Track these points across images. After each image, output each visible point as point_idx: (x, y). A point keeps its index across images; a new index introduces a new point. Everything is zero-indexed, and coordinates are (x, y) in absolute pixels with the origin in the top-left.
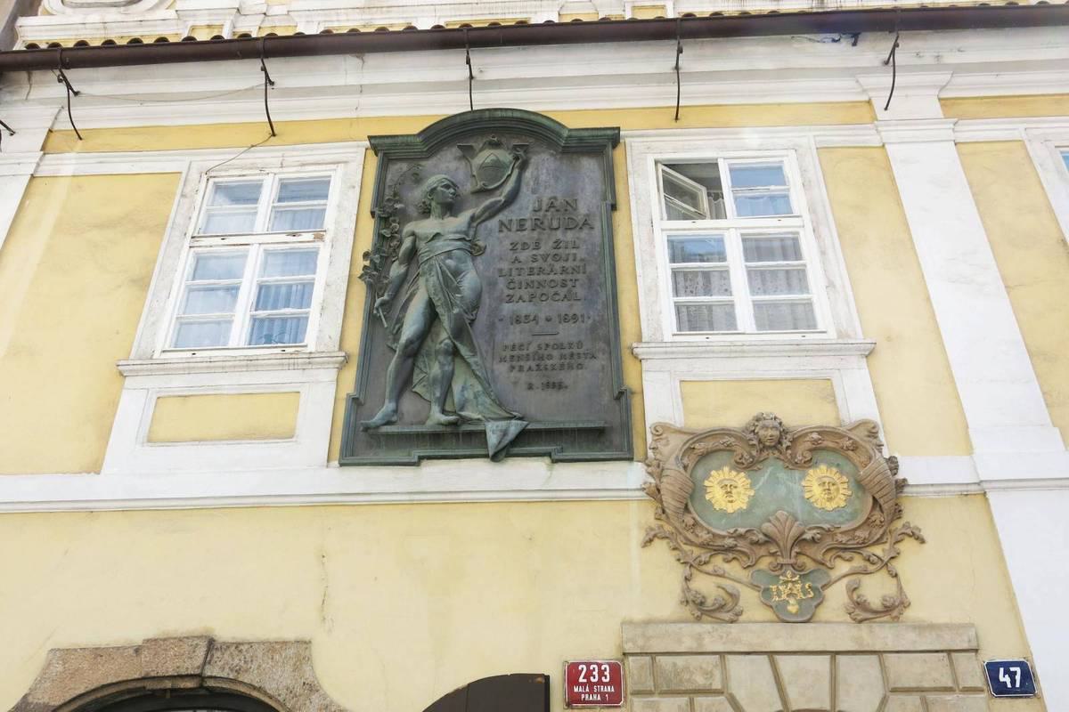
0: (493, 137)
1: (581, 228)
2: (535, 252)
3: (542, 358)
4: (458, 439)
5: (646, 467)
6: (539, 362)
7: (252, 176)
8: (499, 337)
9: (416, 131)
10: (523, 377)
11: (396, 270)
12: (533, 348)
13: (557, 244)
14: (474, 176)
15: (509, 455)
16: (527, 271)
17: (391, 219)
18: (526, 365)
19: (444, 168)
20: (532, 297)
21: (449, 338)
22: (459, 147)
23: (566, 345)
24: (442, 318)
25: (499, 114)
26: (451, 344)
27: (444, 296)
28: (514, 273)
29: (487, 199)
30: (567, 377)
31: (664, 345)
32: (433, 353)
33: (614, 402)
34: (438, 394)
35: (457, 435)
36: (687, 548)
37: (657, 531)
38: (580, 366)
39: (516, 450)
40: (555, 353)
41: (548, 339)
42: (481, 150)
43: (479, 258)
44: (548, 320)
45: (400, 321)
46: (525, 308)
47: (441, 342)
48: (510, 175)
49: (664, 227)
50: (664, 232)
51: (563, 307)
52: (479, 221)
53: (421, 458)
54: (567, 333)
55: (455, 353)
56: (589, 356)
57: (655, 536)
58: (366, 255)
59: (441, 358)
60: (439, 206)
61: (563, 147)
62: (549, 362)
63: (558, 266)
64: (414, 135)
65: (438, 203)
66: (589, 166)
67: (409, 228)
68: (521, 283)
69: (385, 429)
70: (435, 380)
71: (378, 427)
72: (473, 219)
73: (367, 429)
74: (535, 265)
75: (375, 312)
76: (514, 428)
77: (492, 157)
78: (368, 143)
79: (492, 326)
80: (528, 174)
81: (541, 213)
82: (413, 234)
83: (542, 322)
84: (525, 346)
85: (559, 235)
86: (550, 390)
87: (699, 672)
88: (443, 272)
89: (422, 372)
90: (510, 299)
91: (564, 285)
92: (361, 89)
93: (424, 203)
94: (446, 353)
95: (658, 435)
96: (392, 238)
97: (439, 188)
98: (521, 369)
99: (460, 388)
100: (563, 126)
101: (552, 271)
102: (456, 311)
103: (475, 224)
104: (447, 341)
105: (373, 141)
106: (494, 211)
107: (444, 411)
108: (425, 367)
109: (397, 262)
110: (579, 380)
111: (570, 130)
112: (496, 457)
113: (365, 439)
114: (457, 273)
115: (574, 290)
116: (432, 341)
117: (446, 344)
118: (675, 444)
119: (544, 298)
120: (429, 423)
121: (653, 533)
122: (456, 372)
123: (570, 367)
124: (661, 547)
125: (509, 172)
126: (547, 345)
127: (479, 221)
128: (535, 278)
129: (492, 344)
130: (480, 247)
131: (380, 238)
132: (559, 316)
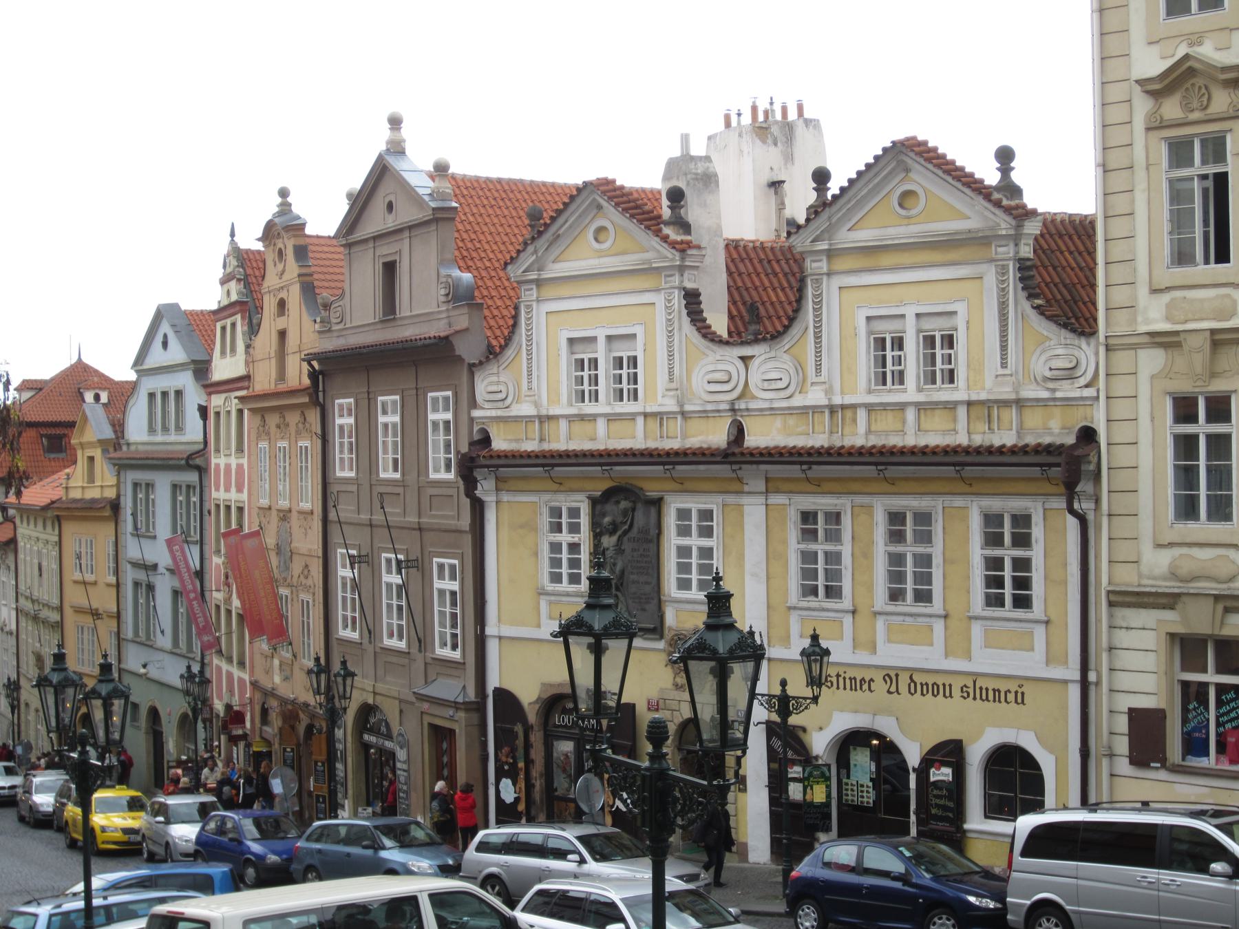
30: (647, 607)
54: (647, 589)
55: (616, 596)
66: (653, 511)
87: (674, 705)
106: (625, 533)
114: (615, 565)
118: (673, 633)
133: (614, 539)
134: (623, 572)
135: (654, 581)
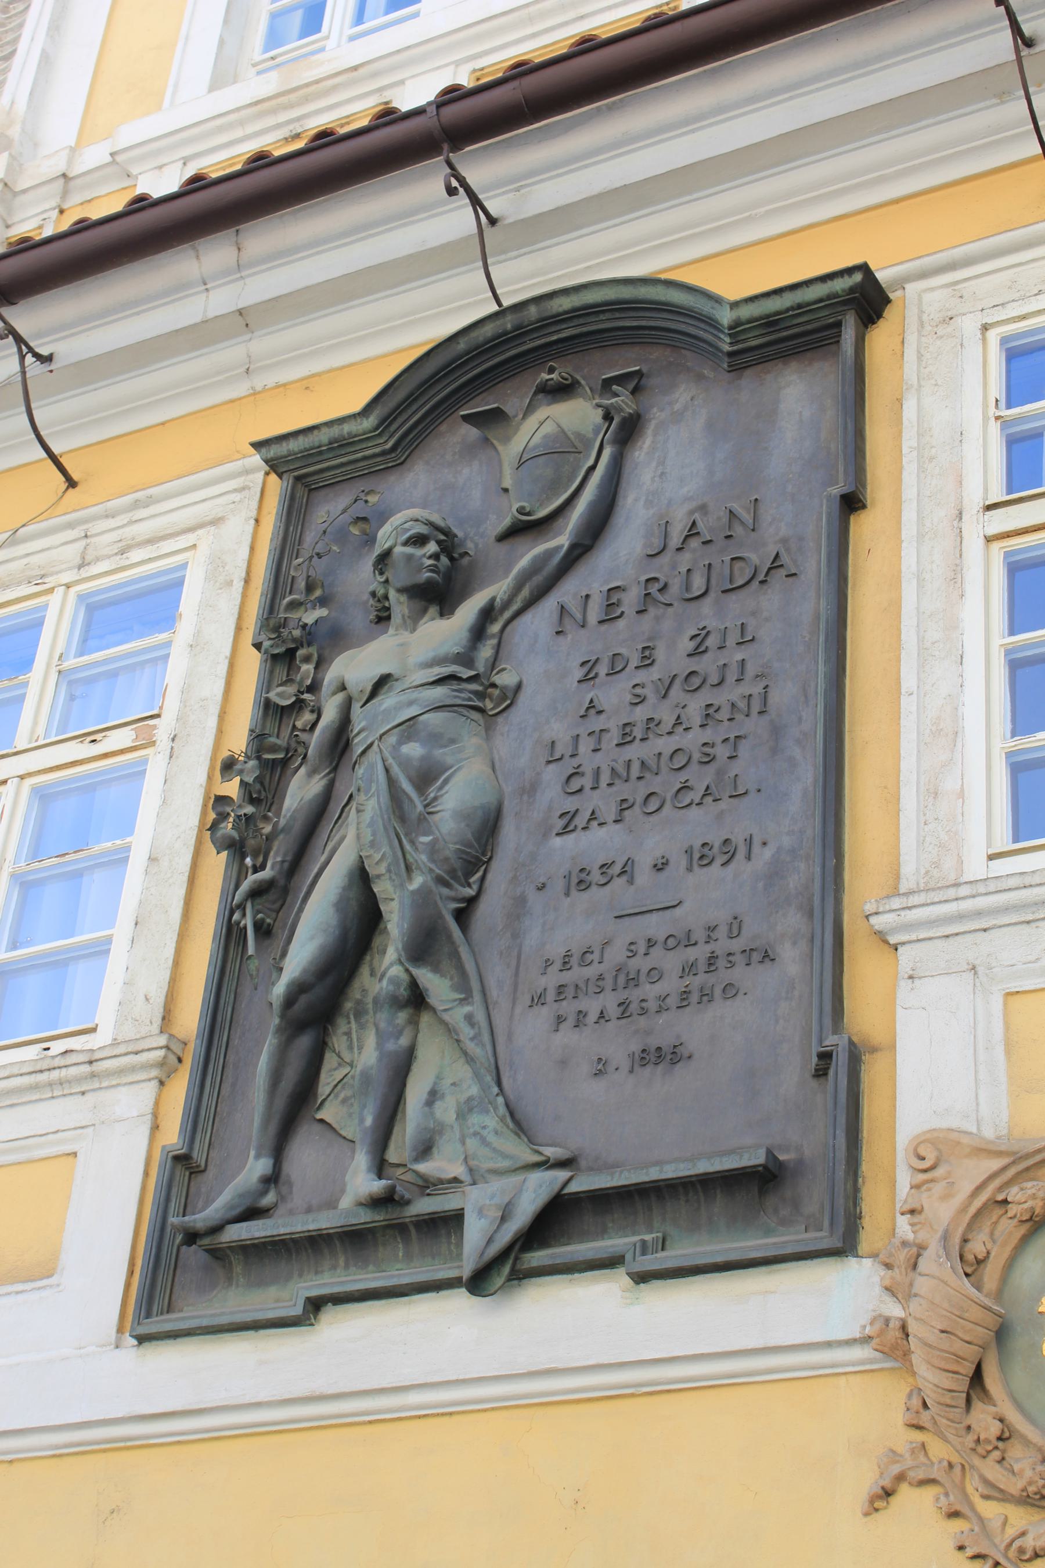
0: (551, 370)
1: (762, 582)
2: (641, 677)
3: (633, 981)
4: (403, 1236)
5: (882, 1271)
6: (622, 995)
7: (144, 566)
8: (532, 939)
9: (358, 406)
11: (301, 790)
12: (616, 954)
13: (700, 638)
14: (506, 490)
15: (520, 1276)
16: (614, 736)
17: (300, 653)
18: (592, 1006)
19: (452, 486)
20: (624, 806)
21: (401, 963)
22: (466, 418)
23: (699, 935)
25: (565, 304)
26: (404, 976)
27: (391, 847)
28: (585, 746)
31: (964, 891)
32: (370, 1006)
33: (814, 1083)
34: (369, 1121)
35: (401, 1229)
36: (990, 1510)
37: (909, 1463)
38: (730, 991)
39: (538, 1257)
40: (671, 962)
41: (656, 926)
42: (529, 410)
43: (500, 719)
44: (660, 867)
46: (598, 843)
48: (593, 468)
49: (992, 531)
50: (996, 546)
51: (698, 825)
52: (507, 615)
53: (316, 1305)
54: (707, 897)
55: (416, 999)
56: (756, 957)
57: (901, 1478)
59: (383, 1017)
60: (403, 598)
61: (730, 354)
62: (650, 991)
64: (354, 416)
65: (400, 591)
66: (797, 394)
68: (597, 772)
70: (366, 1078)
71: (217, 1229)
73: (192, 1237)
74: (640, 714)
77: (548, 428)
78: (256, 459)
79: (518, 907)
80: (642, 452)
81: (665, 559)
83: (644, 876)
84: (596, 956)
85: (707, 613)
86: (648, 1070)
89: (342, 1062)
90: (568, 824)
91: (709, 760)
92: (245, 320)
93: (373, 594)
94: (396, 1003)
95: (925, 1171)
96: (299, 705)
97: (399, 550)
99: (424, 1096)
100: (717, 300)
101: (678, 722)
103: (495, 628)
105: (274, 451)
108: (351, 1048)
109: (303, 770)
110: (751, 1025)
111: (735, 305)
112: (478, 1282)
113: (203, 1260)
114: (427, 777)
115: (735, 768)
116: (372, 974)
117: (393, 981)
119: (653, 806)
120: (346, 1202)
121: (896, 1469)
122: (421, 1053)
123: (706, 996)
124: (917, 1505)
125: (590, 462)
126: (651, 943)
127: (507, 615)
128: (634, 752)
129: (514, 963)
130: (504, 690)
131: (268, 709)
132: (689, 852)
135: (783, 823)
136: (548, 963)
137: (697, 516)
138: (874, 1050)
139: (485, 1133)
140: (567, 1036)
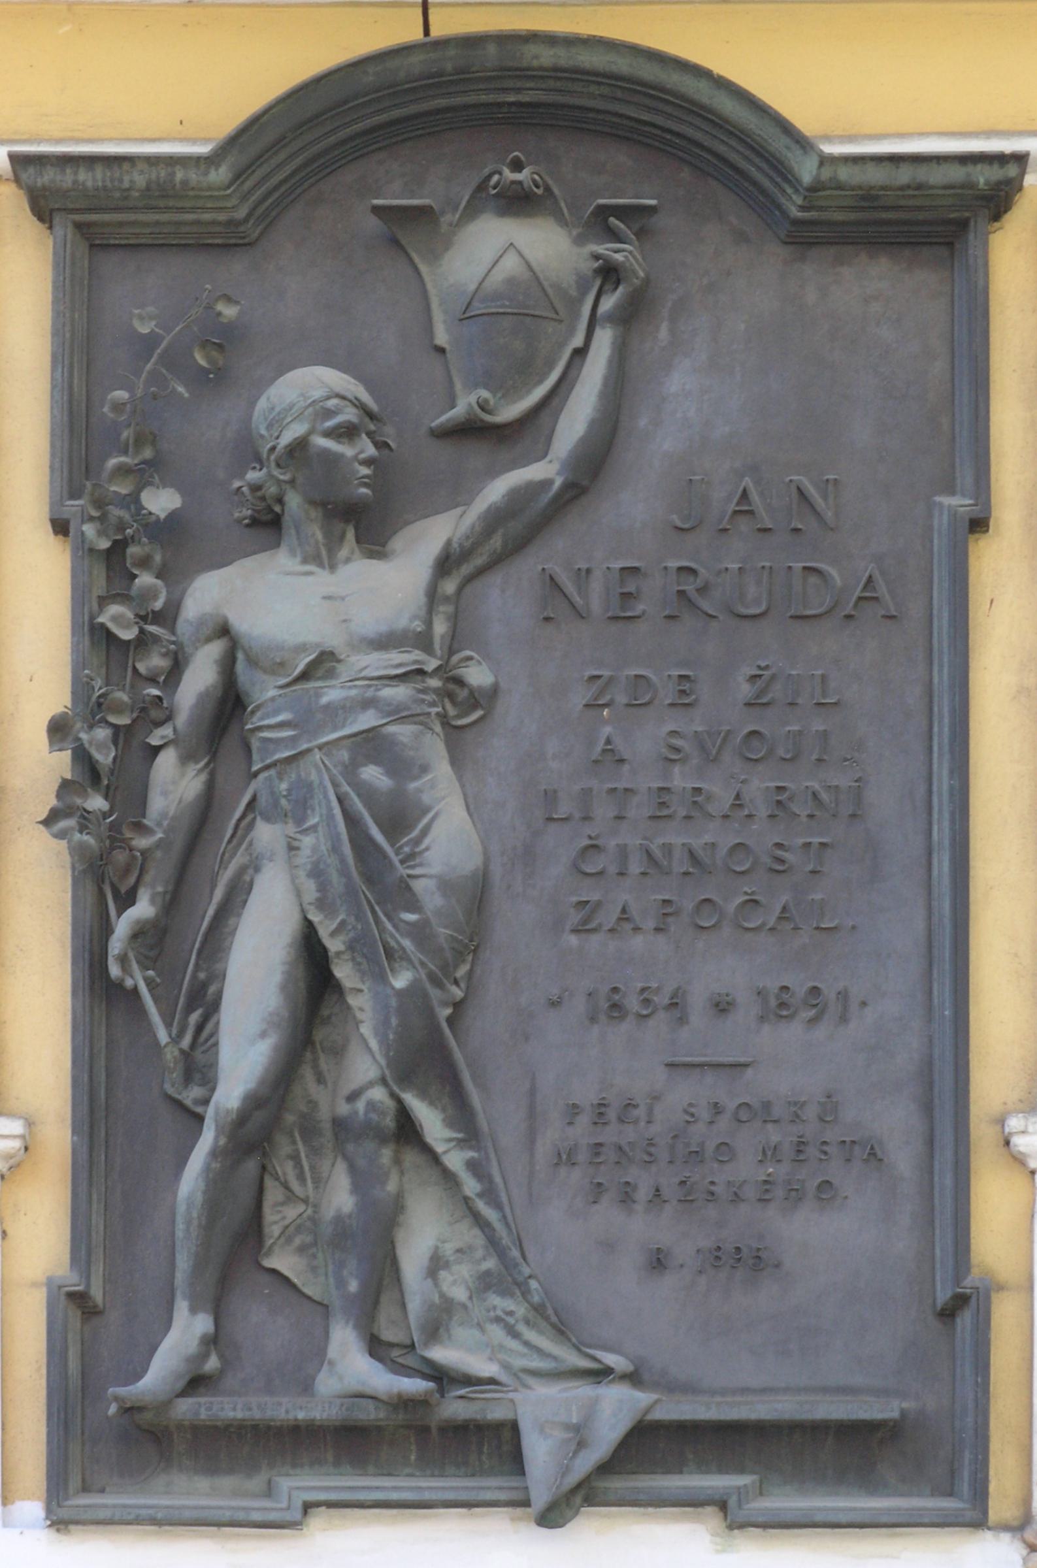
10: (641, 1228)
11: (173, 784)
24: (353, 1001)
28: (603, 811)
29: (493, 473)
34: (353, 1286)
45: (204, 1001)
47: (352, 1097)
52: (466, 569)
54: (790, 1063)
58: (58, 729)
63: (759, 785)
67: (206, 594)
69: (184, 1408)
72: (445, 564)
75: (115, 971)
76: (616, 1408)
82: (224, 631)
88: (352, 820)
96: (143, 642)
98: (627, 1197)
102: (401, 981)
104: (378, 1094)
107: (376, 1347)
133: (387, 587)
134: (476, 896)
136: (574, 1110)
137: (747, 481)
138: (1001, 1288)
139: (511, 1320)
140: (607, 1215)
